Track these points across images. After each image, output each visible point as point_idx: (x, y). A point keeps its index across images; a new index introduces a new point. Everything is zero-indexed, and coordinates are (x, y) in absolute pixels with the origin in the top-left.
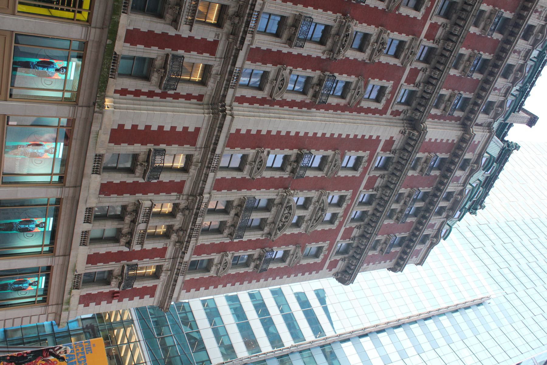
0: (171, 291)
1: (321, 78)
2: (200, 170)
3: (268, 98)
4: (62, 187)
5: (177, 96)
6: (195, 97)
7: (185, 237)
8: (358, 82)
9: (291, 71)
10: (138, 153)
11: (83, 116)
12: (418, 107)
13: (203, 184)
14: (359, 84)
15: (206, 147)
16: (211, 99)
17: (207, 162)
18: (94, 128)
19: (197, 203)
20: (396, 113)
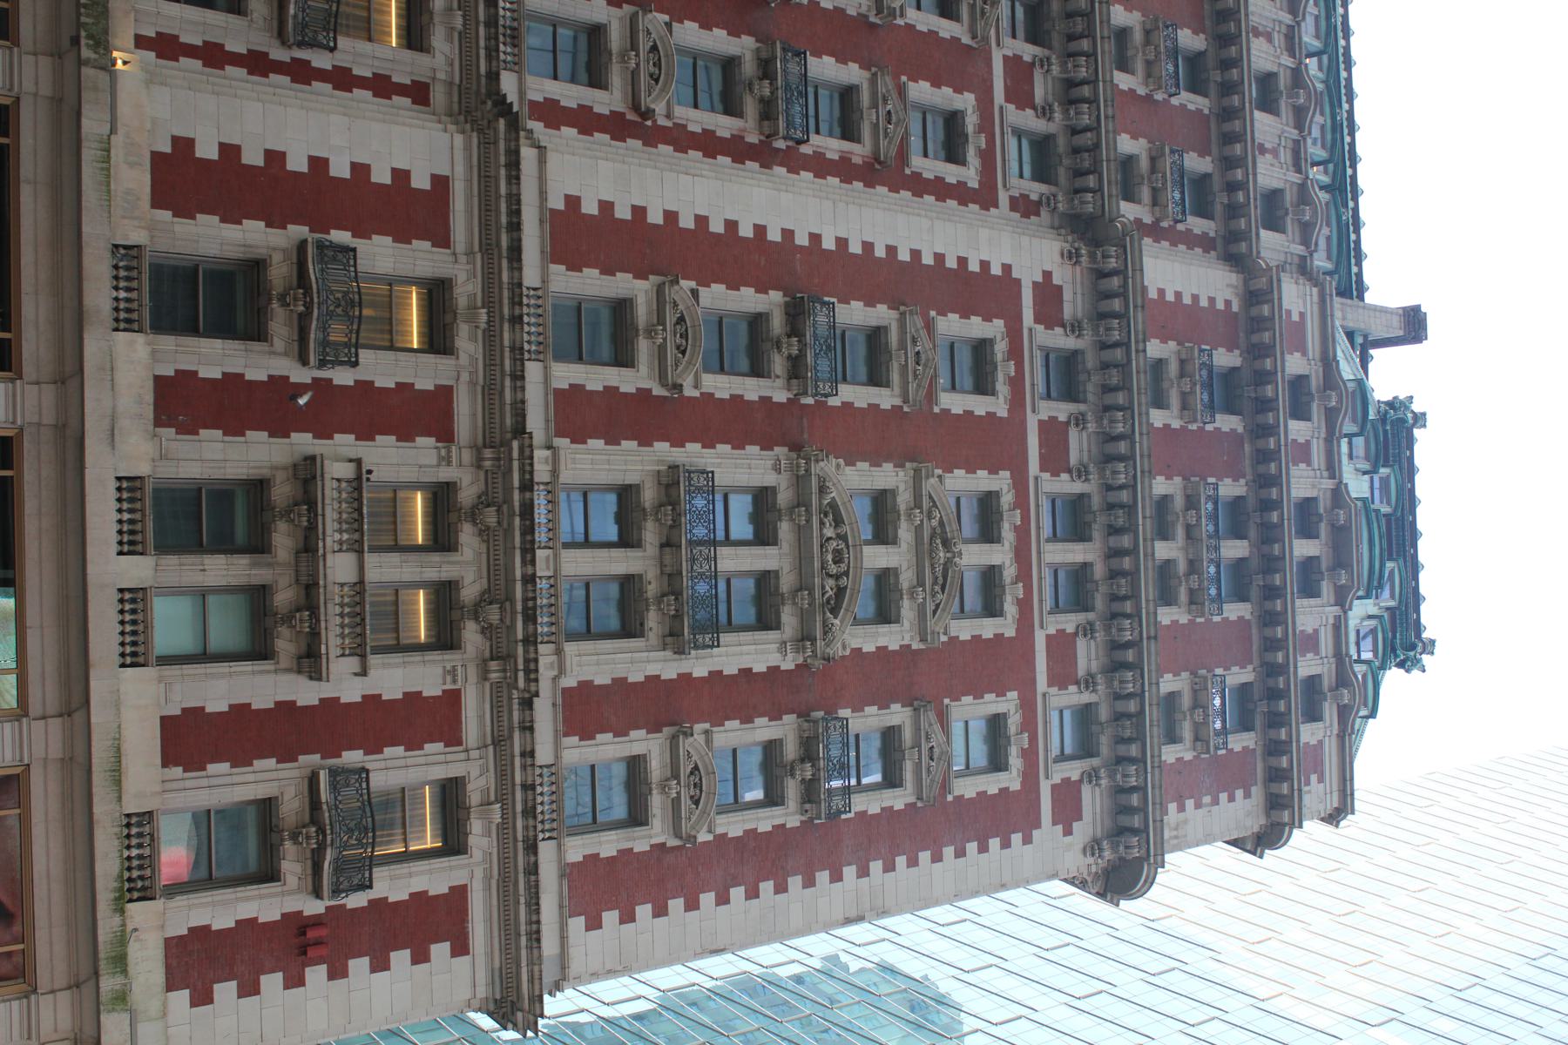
0: (528, 905)
1: (764, 55)
2: (490, 337)
3: (631, 116)
4: (12, 380)
5: (343, 79)
6: (402, 90)
7: (513, 621)
8: (873, 81)
9: (669, 25)
10: (261, 252)
11: (46, 89)
12: (1079, 183)
13: (514, 389)
14: (881, 89)
15: (488, 247)
16: (456, 99)
17: (506, 301)
18: (93, 125)
19: (516, 464)
20: (1025, 207)
